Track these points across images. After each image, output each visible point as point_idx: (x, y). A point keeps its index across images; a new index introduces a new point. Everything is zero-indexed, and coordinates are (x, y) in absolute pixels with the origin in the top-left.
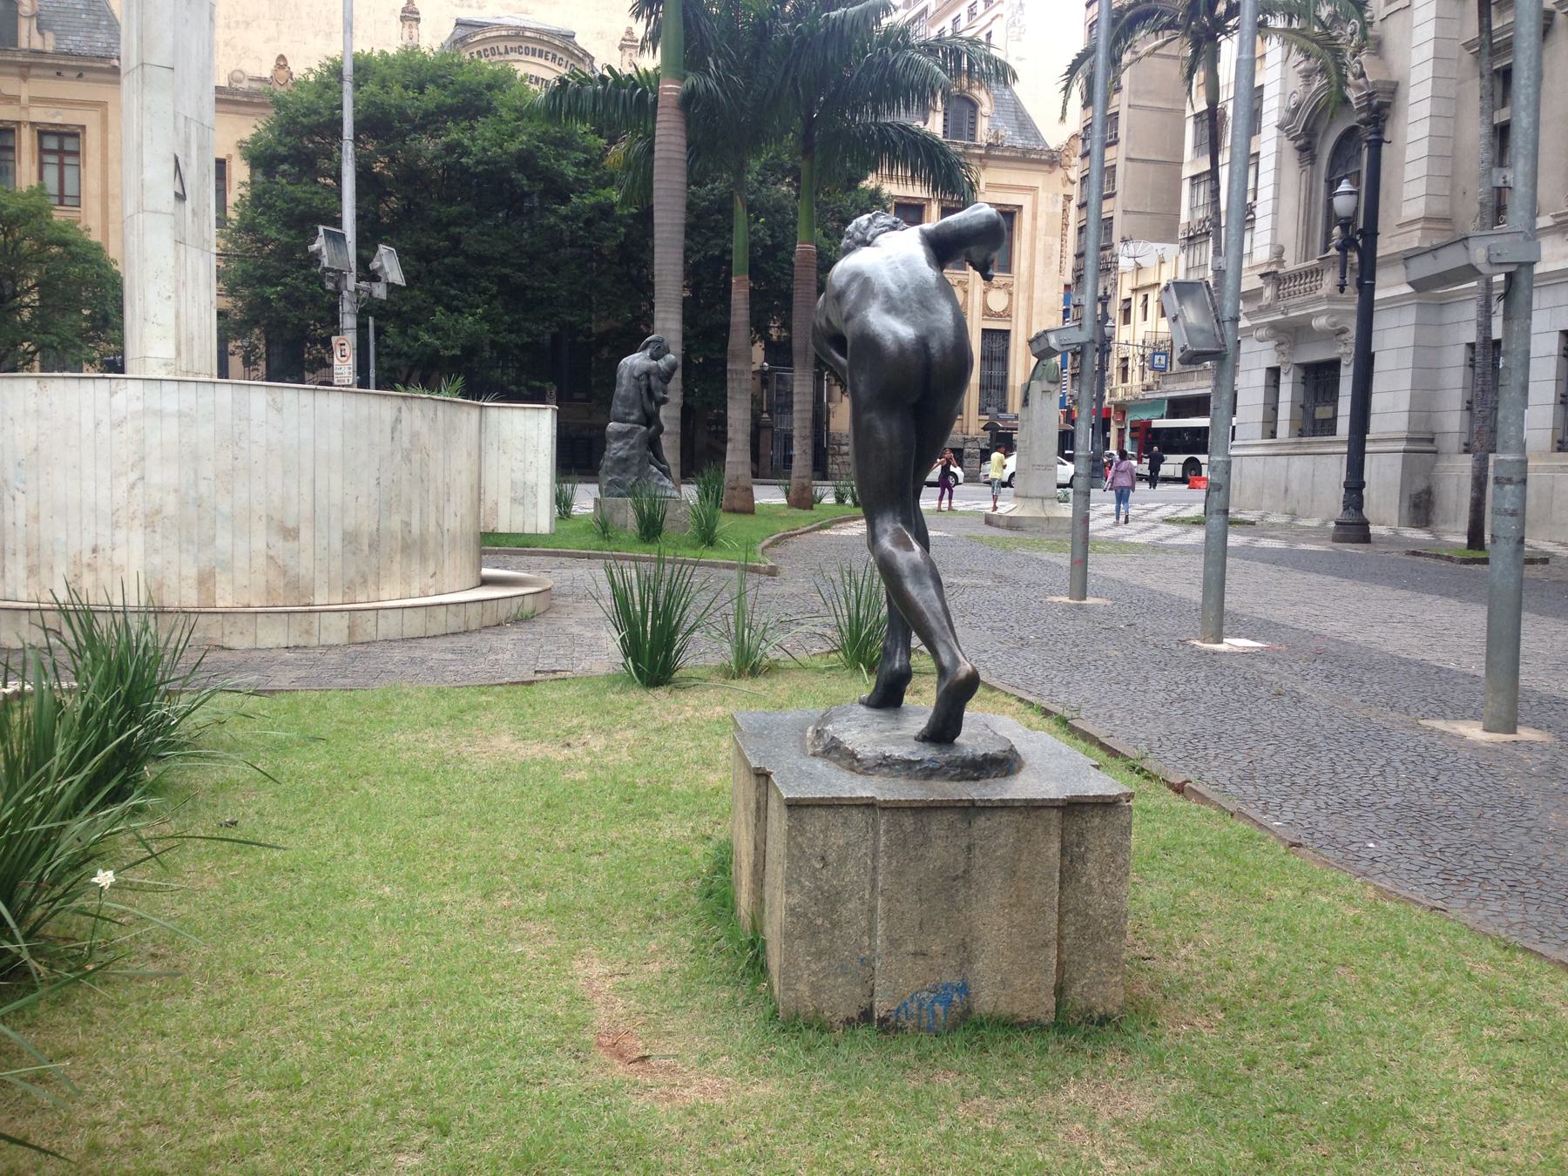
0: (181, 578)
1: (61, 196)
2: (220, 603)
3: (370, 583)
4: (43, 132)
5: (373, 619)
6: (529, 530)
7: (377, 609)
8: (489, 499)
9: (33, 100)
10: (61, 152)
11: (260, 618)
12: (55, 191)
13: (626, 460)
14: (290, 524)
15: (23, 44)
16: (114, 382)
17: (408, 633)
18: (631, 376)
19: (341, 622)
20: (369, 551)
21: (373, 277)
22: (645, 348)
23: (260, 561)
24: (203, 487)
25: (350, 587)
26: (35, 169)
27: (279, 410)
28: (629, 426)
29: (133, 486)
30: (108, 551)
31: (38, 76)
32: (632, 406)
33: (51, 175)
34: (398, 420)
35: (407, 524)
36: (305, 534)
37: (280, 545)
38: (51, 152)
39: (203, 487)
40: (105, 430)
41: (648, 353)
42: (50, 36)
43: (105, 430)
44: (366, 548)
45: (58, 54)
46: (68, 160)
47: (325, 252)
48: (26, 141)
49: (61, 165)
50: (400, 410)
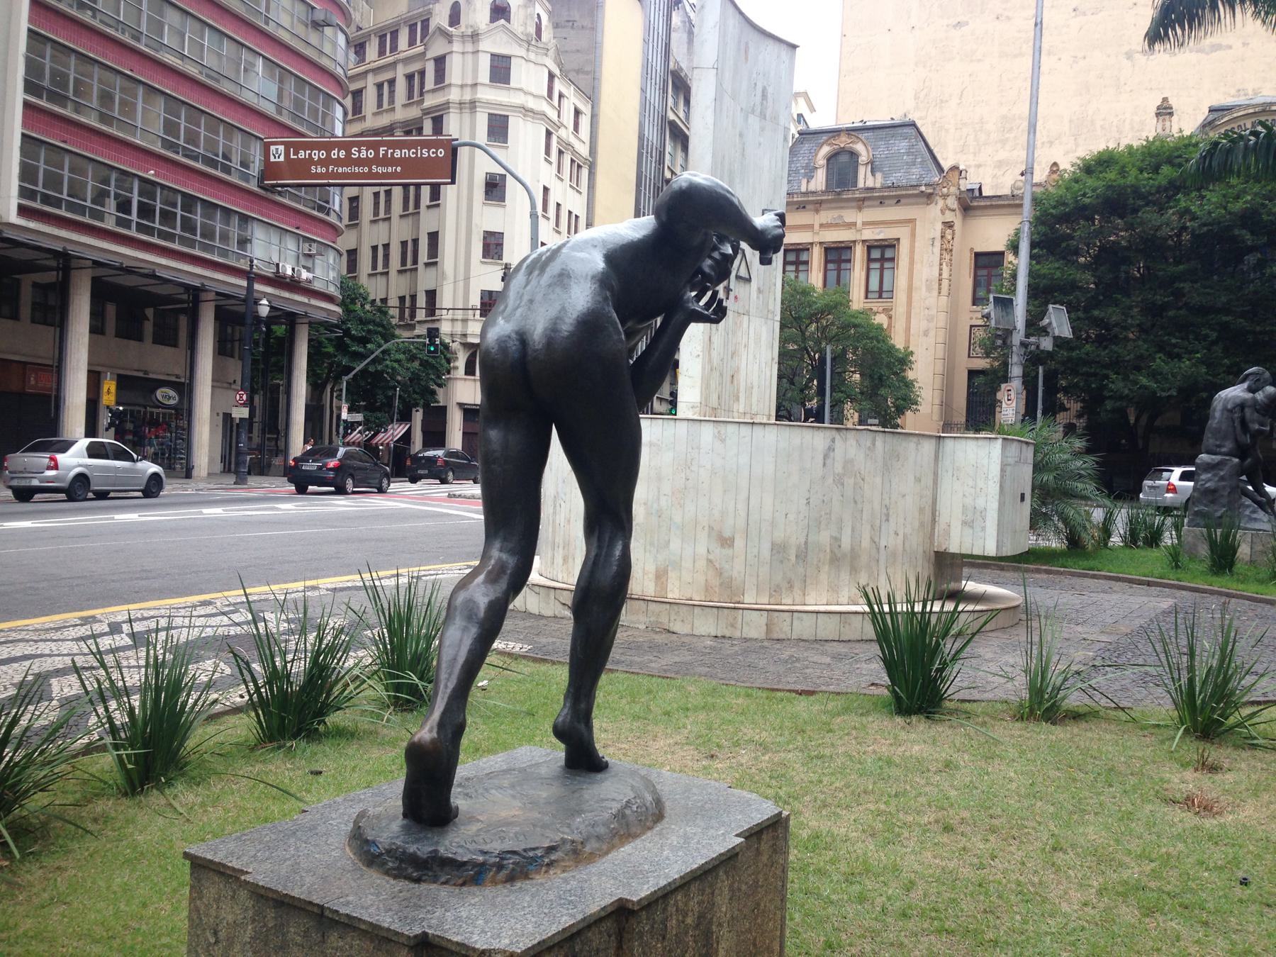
0: (644, 574)
1: (881, 292)
2: (670, 595)
3: (796, 589)
4: (870, 246)
5: (789, 620)
6: (977, 552)
7: (793, 612)
8: (943, 519)
9: (864, 224)
11: (697, 610)
13: (1214, 491)
14: (727, 534)
15: (861, 184)
17: (822, 635)
18: (1225, 409)
19: (761, 619)
20: (795, 562)
21: (1044, 331)
22: (1243, 381)
23: (702, 564)
24: (664, 502)
25: (776, 590)
26: (864, 274)
27: (723, 441)
28: (1218, 458)
31: (869, 207)
32: (1225, 438)
34: (831, 449)
35: (837, 539)
36: (739, 543)
37: (718, 552)
38: (875, 260)
39: (664, 502)
41: (1245, 385)
42: (879, 175)
44: (793, 558)
45: (884, 188)
46: (887, 265)
47: (993, 315)
48: (859, 253)
49: (882, 269)
50: (833, 440)
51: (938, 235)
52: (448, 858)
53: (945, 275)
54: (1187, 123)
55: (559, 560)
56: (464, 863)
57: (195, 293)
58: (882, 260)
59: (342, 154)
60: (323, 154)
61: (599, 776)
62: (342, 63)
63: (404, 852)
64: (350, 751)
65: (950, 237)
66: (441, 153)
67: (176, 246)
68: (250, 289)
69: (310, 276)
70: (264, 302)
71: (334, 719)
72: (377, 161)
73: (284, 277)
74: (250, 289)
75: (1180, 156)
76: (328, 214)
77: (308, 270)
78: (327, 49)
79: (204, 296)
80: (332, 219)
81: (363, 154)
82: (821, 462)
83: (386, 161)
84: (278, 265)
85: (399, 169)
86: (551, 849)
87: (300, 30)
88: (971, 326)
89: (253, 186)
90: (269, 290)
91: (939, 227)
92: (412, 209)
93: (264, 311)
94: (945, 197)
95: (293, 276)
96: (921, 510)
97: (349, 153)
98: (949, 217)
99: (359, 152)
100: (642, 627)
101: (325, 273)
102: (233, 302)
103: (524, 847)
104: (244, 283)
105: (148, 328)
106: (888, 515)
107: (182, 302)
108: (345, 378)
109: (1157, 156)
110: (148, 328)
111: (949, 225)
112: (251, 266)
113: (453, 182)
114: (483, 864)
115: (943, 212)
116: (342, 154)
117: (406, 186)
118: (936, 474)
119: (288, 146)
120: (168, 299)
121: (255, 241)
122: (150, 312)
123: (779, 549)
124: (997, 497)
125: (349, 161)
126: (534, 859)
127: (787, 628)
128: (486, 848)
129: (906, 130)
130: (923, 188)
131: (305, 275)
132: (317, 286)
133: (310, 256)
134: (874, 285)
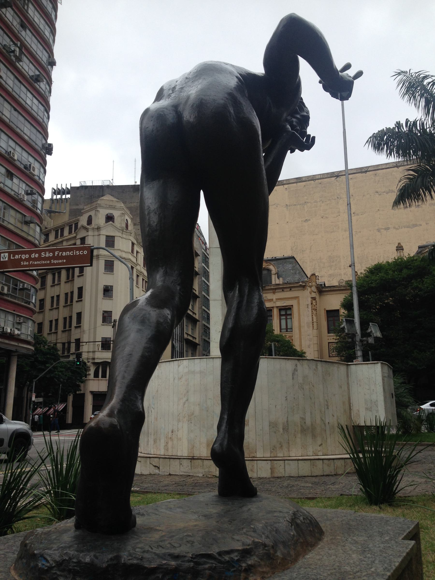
1: (287, 329)
4: (281, 309)
5: (283, 465)
7: (284, 460)
8: (355, 408)
9: (277, 299)
10: (286, 315)
12: (285, 328)
15: (273, 283)
16: (179, 361)
17: (301, 473)
21: (369, 335)
29: (184, 404)
30: (176, 431)
31: (278, 292)
33: (283, 322)
34: (295, 370)
35: (303, 419)
38: (283, 315)
40: (176, 381)
42: (281, 279)
43: (176, 381)
44: (281, 430)
45: (284, 284)
46: (288, 317)
47: (346, 327)
48: (275, 312)
49: (286, 319)
51: (310, 303)
52: (132, 565)
53: (315, 320)
54: (411, 251)
55: (151, 442)
56: (153, 571)
58: (286, 315)
59: (37, 255)
60: (27, 256)
61: (254, 499)
62: (38, 239)
63: (79, 562)
65: (315, 304)
66: (85, 252)
69: (19, 332)
72: (54, 258)
73: (6, 333)
75: (410, 265)
76: (29, 304)
77: (19, 330)
78: (31, 233)
80: (31, 306)
81: (47, 255)
82: (292, 378)
84: (3, 328)
86: (246, 553)
87: (19, 225)
88: (329, 343)
91: (310, 299)
92: (70, 279)
94: (311, 287)
95: (11, 333)
96: (344, 403)
97: (40, 255)
98: (314, 295)
99: (45, 254)
100: (201, 475)
101: (27, 331)
106: (327, 405)
108: (35, 380)
109: (400, 265)
111: (314, 299)
113: (91, 265)
114: (176, 570)
115: (310, 293)
116: (37, 255)
117: (68, 269)
118: (348, 384)
119: (10, 253)
123: (273, 425)
124: (382, 394)
125: (40, 259)
126: (230, 563)
127: (282, 470)
128: (176, 551)
129: (291, 260)
130: (301, 283)
131: (17, 332)
132: (23, 337)
133: (19, 323)
134: (284, 326)
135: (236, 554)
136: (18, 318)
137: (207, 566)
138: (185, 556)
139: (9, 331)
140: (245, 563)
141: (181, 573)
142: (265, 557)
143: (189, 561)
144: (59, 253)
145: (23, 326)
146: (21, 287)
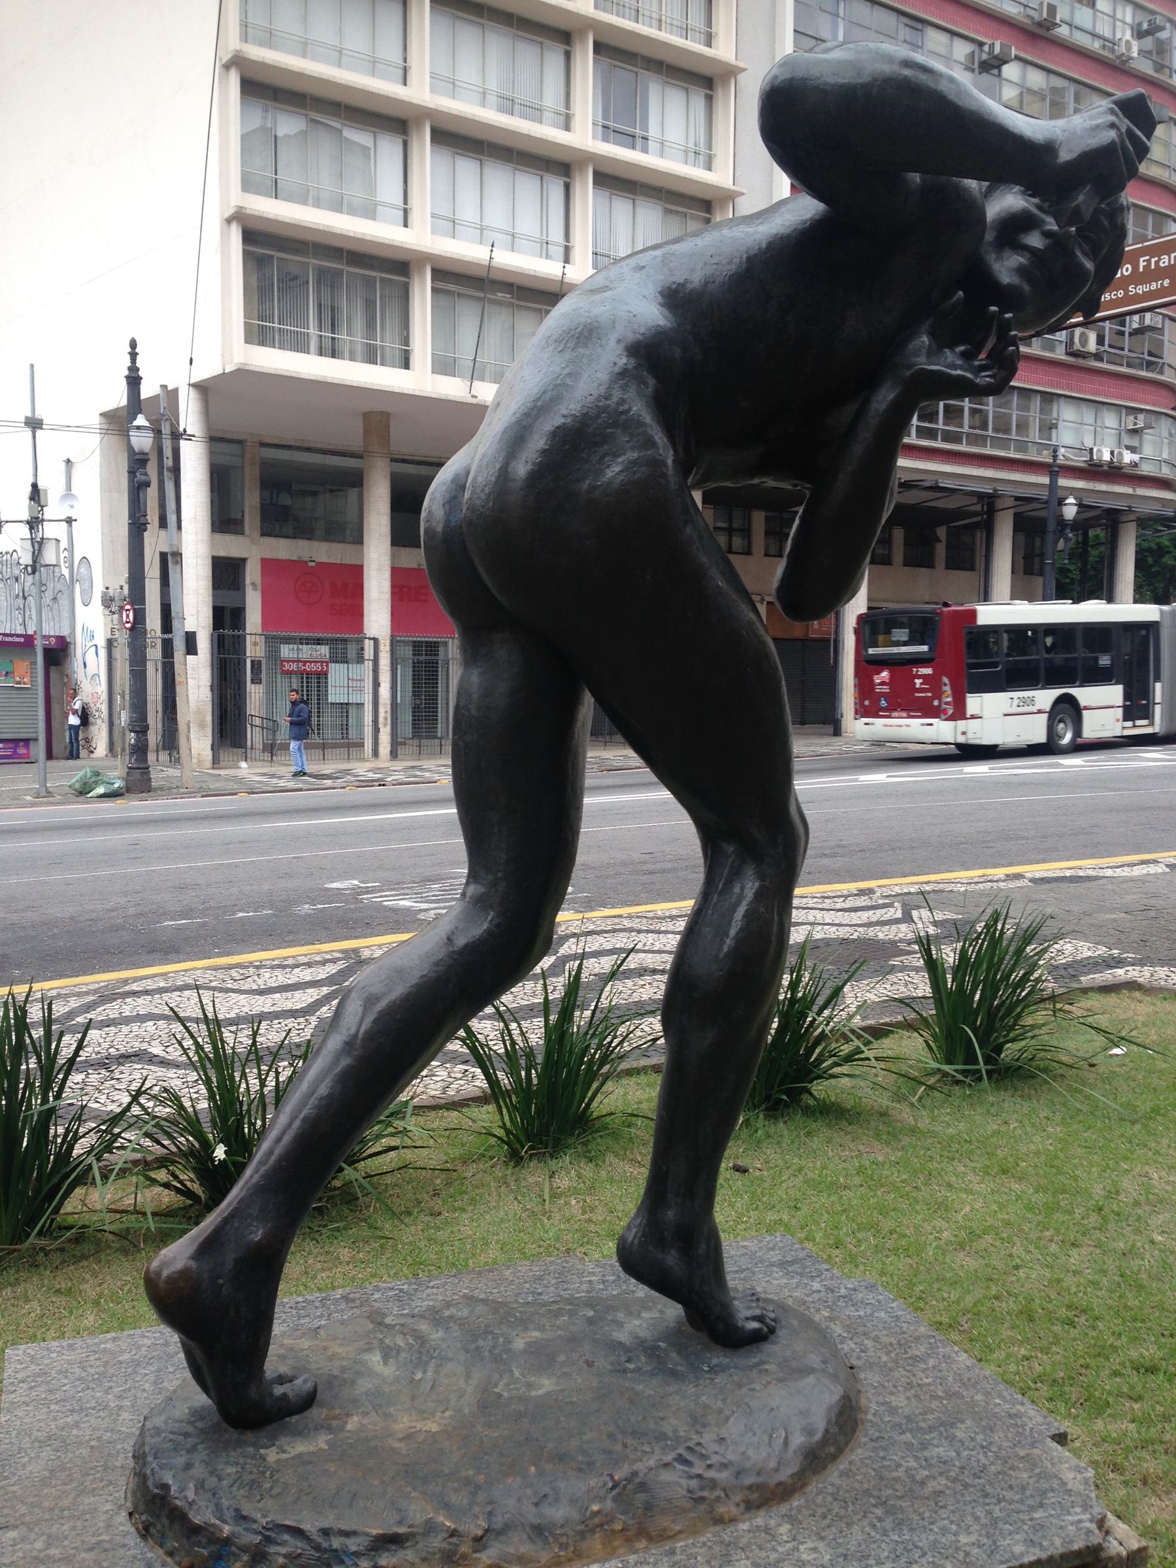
57: (989, 502)
64: (815, 1143)
67: (963, 448)
68: (1053, 483)
69: (1136, 457)
70: (1071, 500)
71: (819, 1088)
74: (1053, 486)
77: (1133, 449)
79: (1000, 504)
83: (1159, 273)
84: (1091, 450)
85: (1166, 283)
89: (1060, 354)
90: (1080, 484)
93: (1070, 511)
95: (1111, 462)
102: (1036, 505)
103: (329, 1521)
104: (1046, 480)
105: (941, 550)
107: (975, 514)
110: (941, 550)
112: (1055, 457)
120: (959, 514)
121: (1061, 424)
122: (942, 532)
131: (1128, 457)
132: (1147, 469)
133: (1135, 432)
135: (358, 1540)
136: (1131, 418)
137: (283, 1550)
138: (255, 1521)
139: (1107, 457)
140: (372, 1560)
141: (233, 1548)
142: (437, 1557)
143: (258, 1533)
144: (1149, 261)
145: (1148, 437)
146: (1135, 326)
